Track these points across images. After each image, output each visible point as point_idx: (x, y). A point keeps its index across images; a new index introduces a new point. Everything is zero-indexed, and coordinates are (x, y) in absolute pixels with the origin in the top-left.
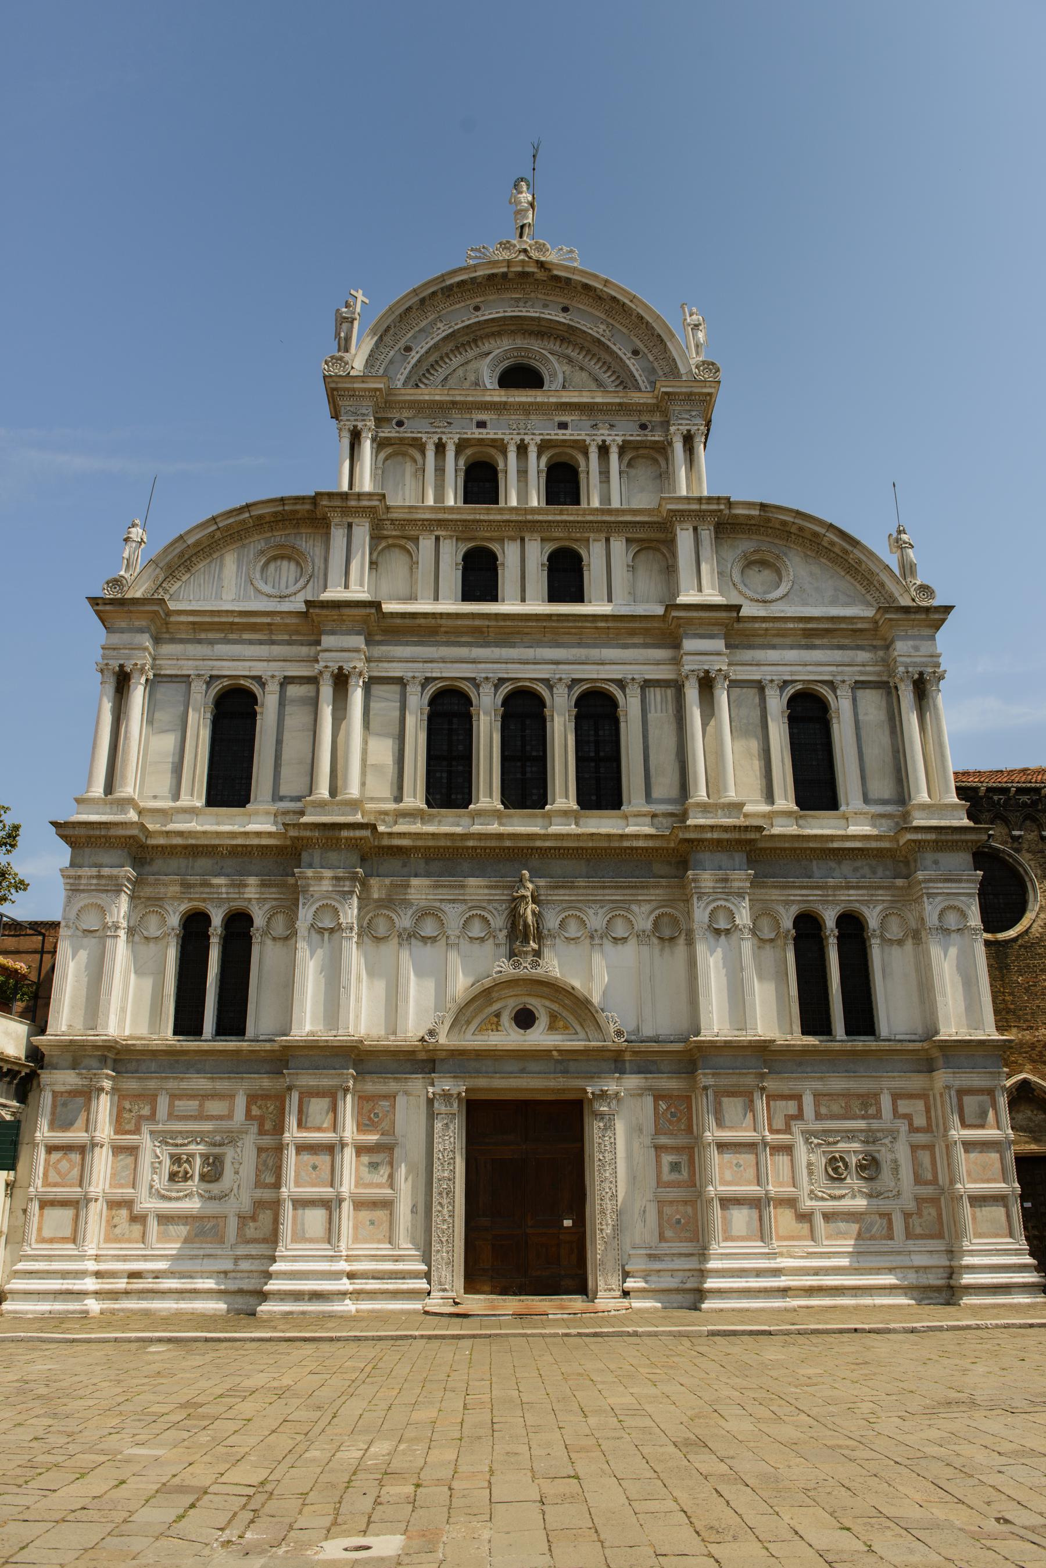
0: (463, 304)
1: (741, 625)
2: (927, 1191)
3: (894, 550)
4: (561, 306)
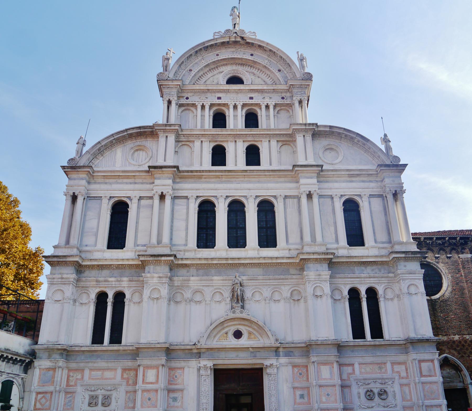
1: (323, 173)
2: (408, 404)
3: (383, 143)
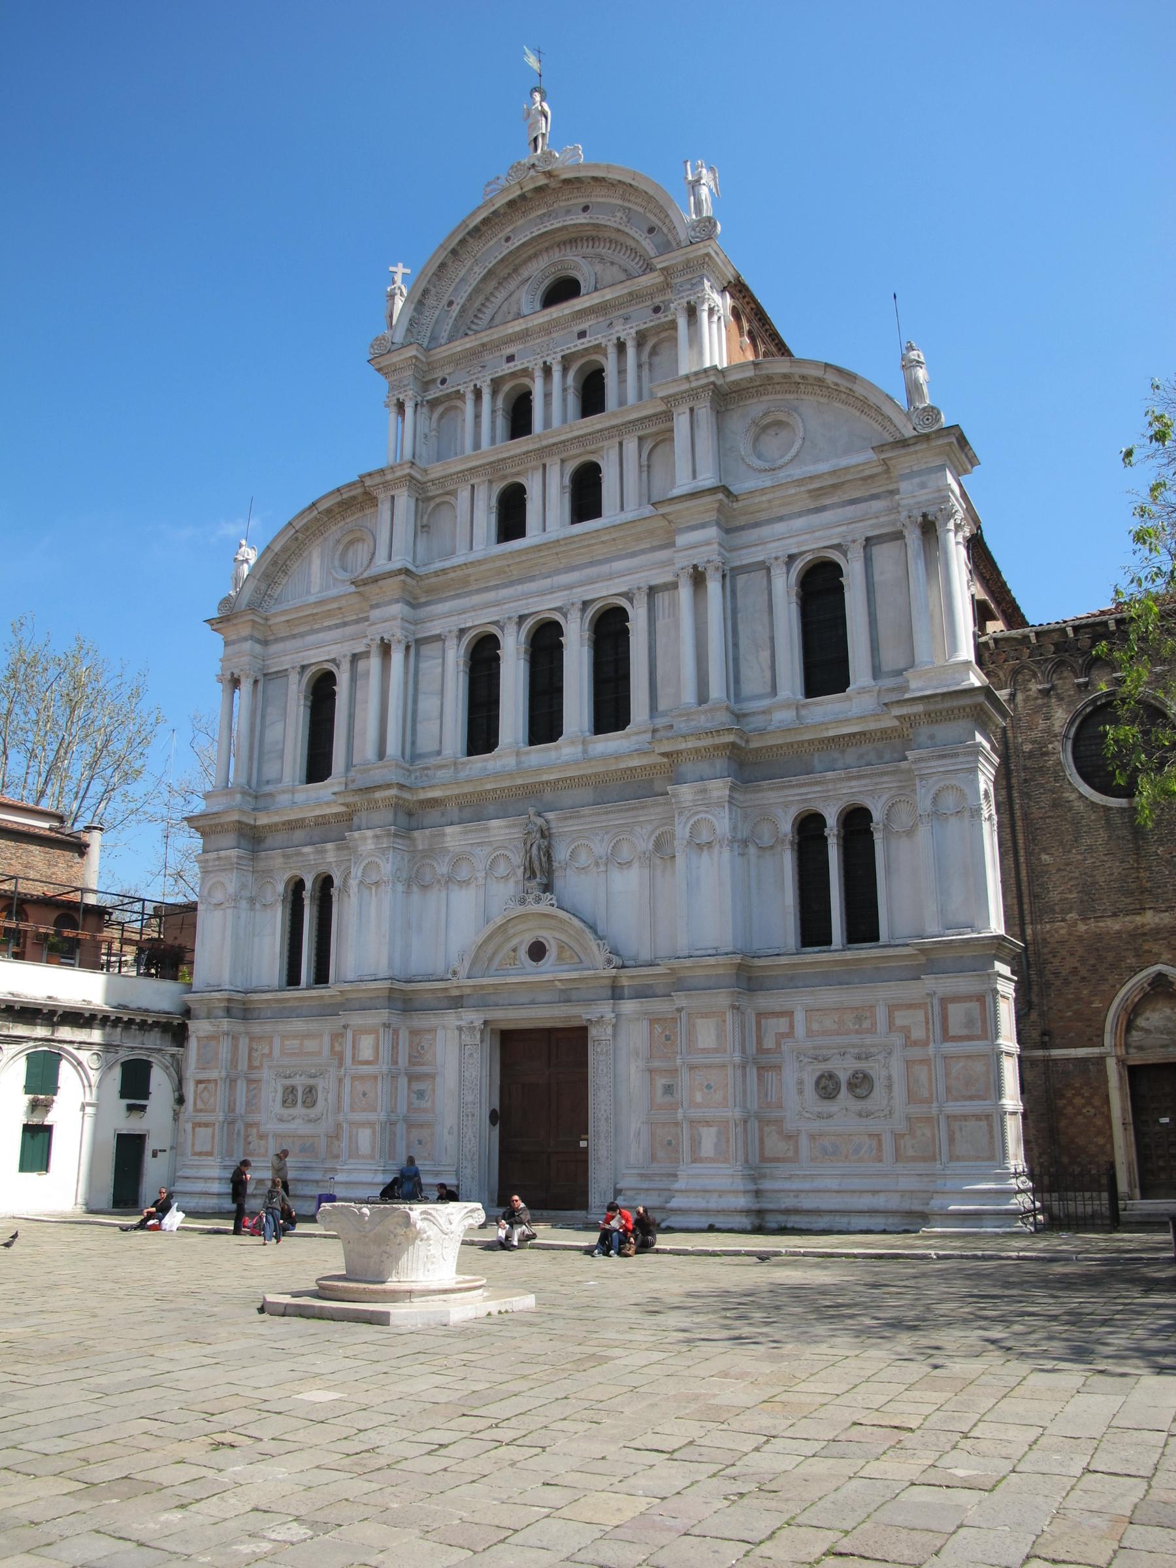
0: (495, 240)
1: (740, 504)
4: (581, 207)
